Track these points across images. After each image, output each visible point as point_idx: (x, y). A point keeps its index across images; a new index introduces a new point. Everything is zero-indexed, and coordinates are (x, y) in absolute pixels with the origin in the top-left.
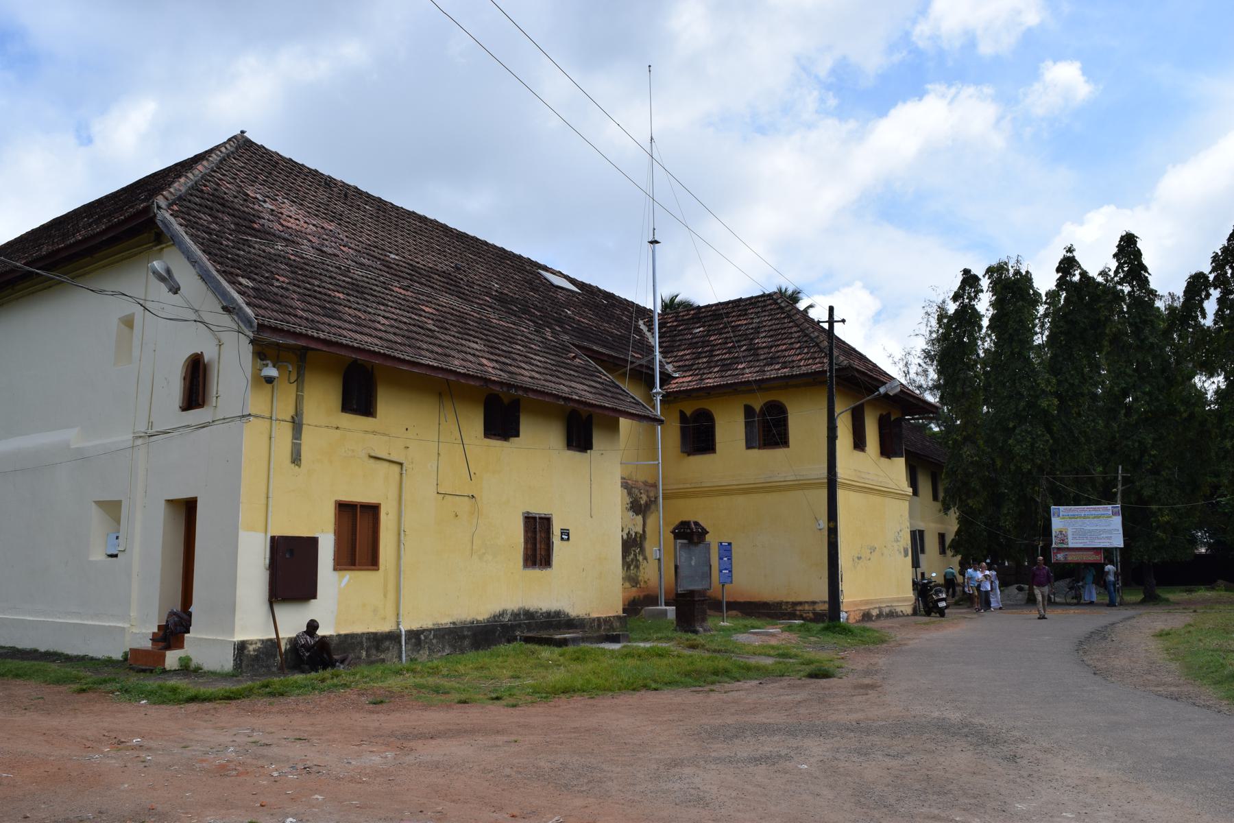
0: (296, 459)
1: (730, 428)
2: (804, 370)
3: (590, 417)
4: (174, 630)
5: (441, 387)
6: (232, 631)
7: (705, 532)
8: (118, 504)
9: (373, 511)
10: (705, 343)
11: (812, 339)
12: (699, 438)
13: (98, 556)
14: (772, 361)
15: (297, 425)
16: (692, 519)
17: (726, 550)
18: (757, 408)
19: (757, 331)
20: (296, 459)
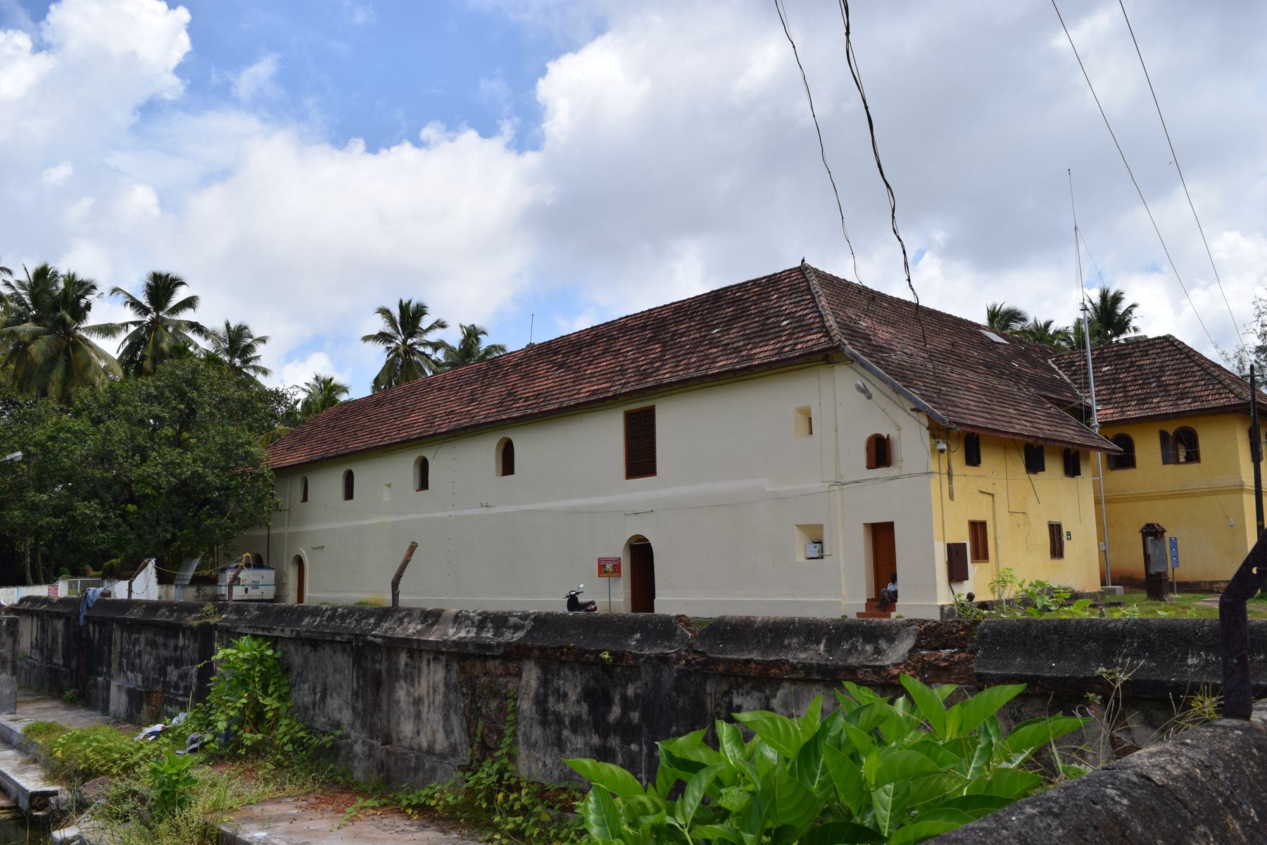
0: (951, 497)
1: (1148, 449)
2: (1213, 404)
3: (1077, 453)
4: (883, 600)
5: (1006, 442)
6: (936, 600)
7: (1164, 531)
8: (820, 527)
9: (983, 525)
10: (1116, 381)
11: (1215, 378)
12: (1123, 459)
13: (801, 558)
14: (1183, 396)
15: (950, 474)
16: (1154, 521)
17: (1174, 543)
18: (1171, 432)
19: (1162, 369)
20: (951, 497)
